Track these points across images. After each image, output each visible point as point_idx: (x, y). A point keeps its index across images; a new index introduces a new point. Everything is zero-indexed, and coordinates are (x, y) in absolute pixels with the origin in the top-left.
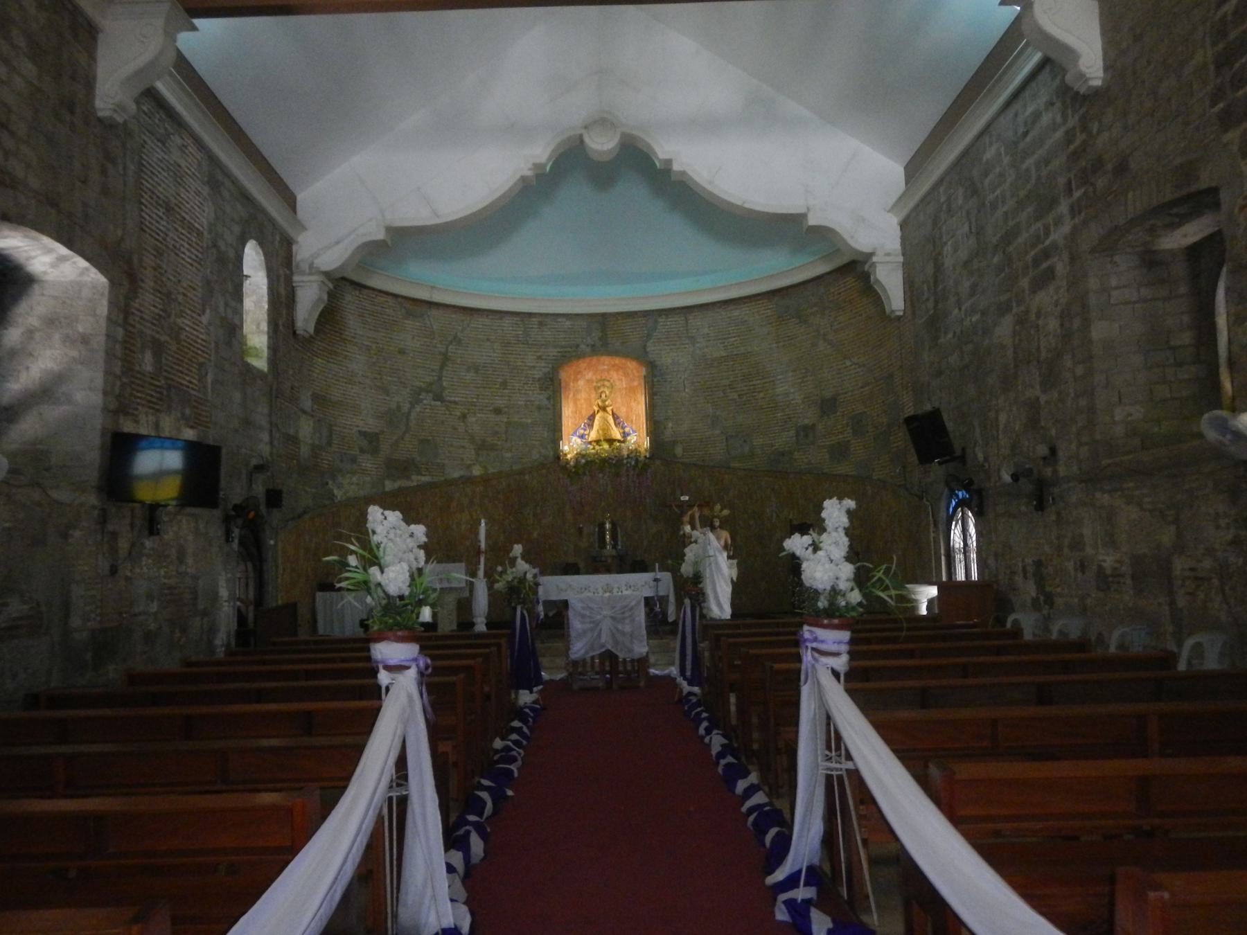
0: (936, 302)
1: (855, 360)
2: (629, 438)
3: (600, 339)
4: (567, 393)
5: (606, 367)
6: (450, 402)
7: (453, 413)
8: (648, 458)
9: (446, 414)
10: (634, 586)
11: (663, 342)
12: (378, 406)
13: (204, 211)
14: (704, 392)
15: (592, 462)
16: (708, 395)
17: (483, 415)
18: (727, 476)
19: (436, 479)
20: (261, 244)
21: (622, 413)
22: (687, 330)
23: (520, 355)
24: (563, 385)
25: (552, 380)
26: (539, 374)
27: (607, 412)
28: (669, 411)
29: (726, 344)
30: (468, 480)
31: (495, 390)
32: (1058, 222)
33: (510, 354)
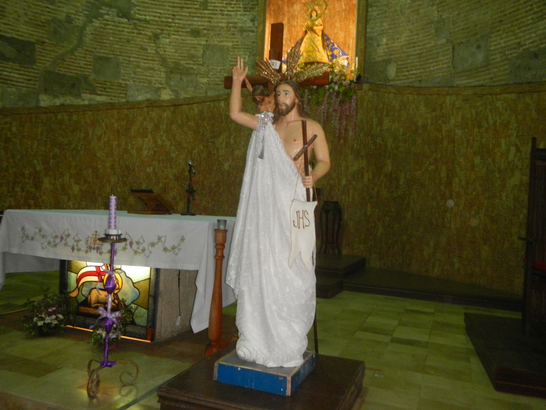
6: (139, 20)
7: (142, 32)
8: (355, 83)
9: (133, 33)
10: (138, 243)
12: (36, 13)
19: (115, 100)
27: (314, 32)
28: (384, 24)
30: (152, 104)
31: (194, 11)
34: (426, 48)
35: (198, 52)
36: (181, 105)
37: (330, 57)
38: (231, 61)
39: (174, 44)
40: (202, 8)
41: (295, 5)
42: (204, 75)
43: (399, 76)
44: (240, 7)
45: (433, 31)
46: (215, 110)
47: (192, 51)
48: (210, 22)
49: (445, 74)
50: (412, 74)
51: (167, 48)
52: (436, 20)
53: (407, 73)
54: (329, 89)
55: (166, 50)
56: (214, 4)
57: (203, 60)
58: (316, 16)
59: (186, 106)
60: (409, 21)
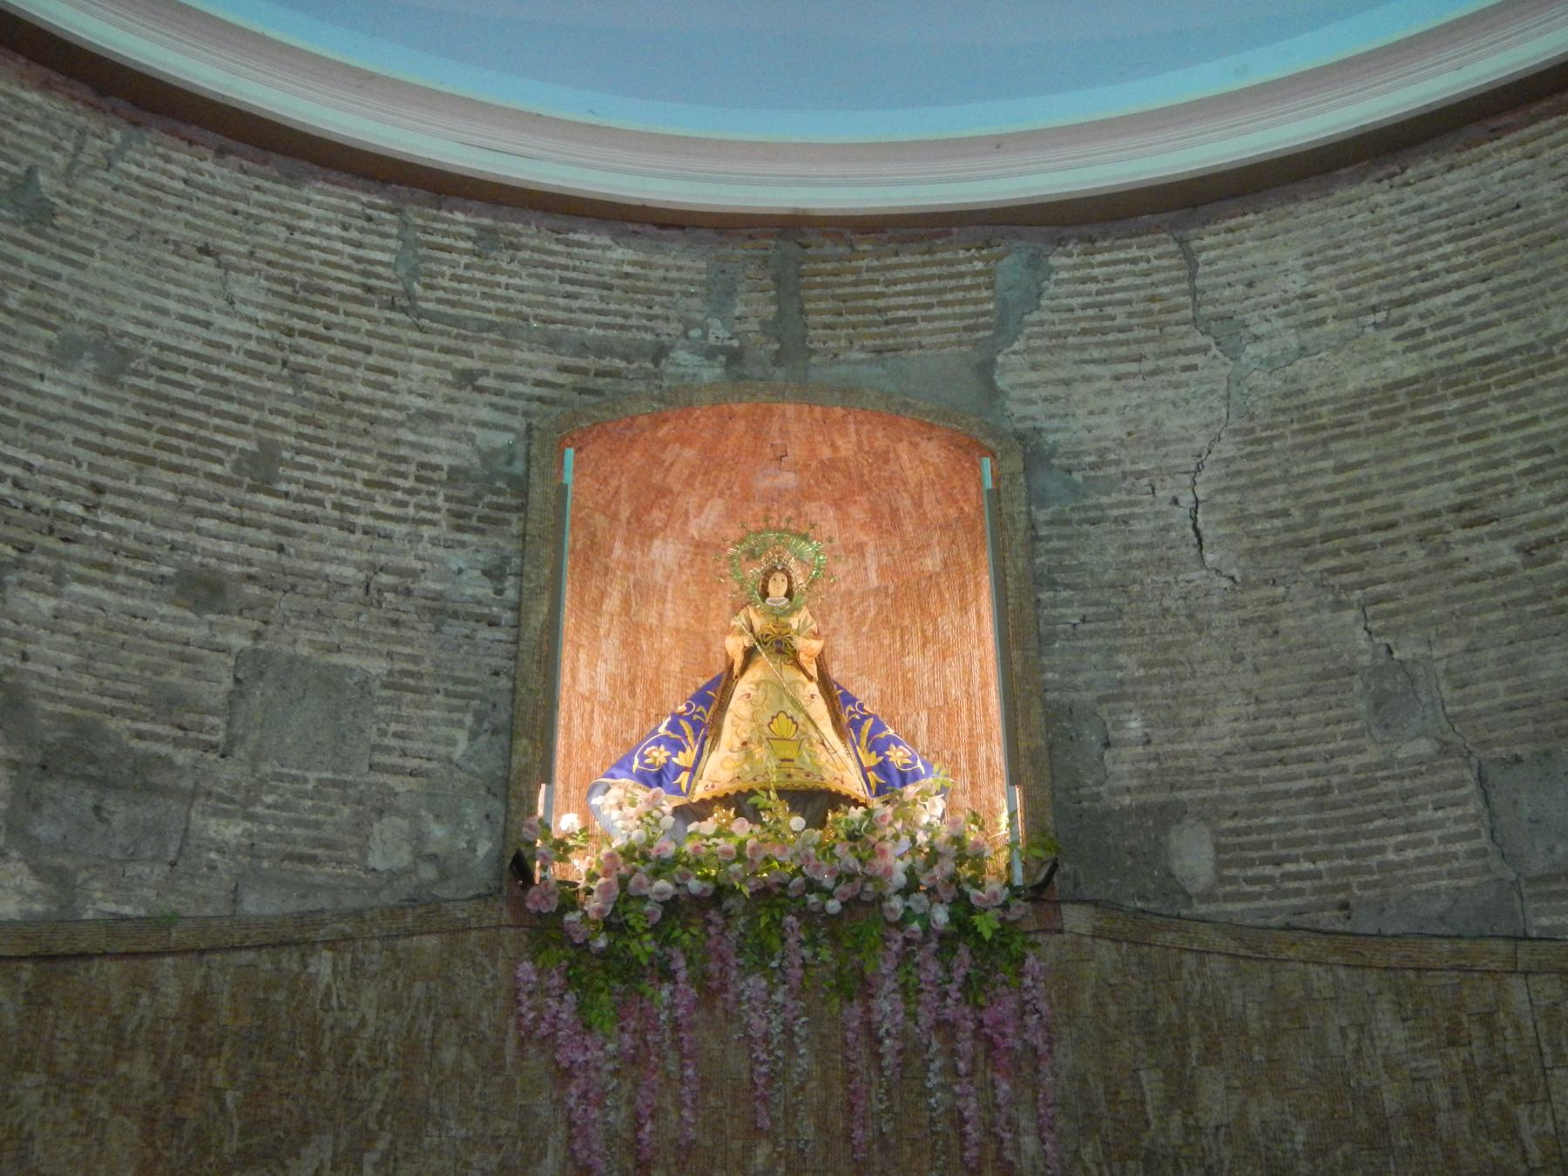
2: (911, 790)
3: (770, 328)
4: (595, 584)
5: (788, 479)
11: (1082, 348)
14: (1308, 559)
15: (721, 892)
16: (1334, 571)
17: (107, 596)
18: (1518, 995)
21: (868, 692)
22: (1194, 292)
23: (368, 351)
24: (572, 539)
25: (520, 486)
26: (449, 452)
28: (1122, 659)
29: (1415, 323)
31: (202, 485)
33: (314, 337)
34: (1344, 770)
35: (203, 684)
36: (84, 956)
37: (872, 776)
38: (375, 748)
39: (79, 627)
40: (247, 480)
41: (657, 543)
42: (231, 801)
43: (1233, 880)
44: (435, 509)
45: (1361, 706)
46: (280, 996)
47: (176, 677)
48: (281, 549)
49: (1467, 882)
50: (1300, 876)
51: (37, 641)
52: (1367, 663)
53: (1269, 870)
54: (901, 924)
55: (30, 648)
56: (308, 476)
57: (229, 724)
58: (789, 594)
59: (113, 968)
60: (1240, 659)
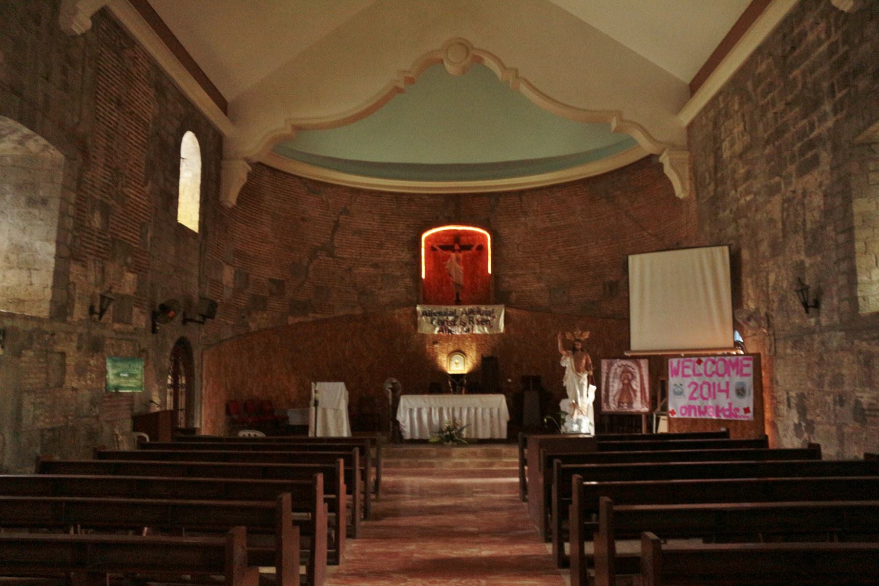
0: (717, 186)
1: (650, 231)
6: (338, 257)
7: (342, 266)
13: (150, 108)
19: (327, 316)
20: (198, 136)
32: (823, 119)
